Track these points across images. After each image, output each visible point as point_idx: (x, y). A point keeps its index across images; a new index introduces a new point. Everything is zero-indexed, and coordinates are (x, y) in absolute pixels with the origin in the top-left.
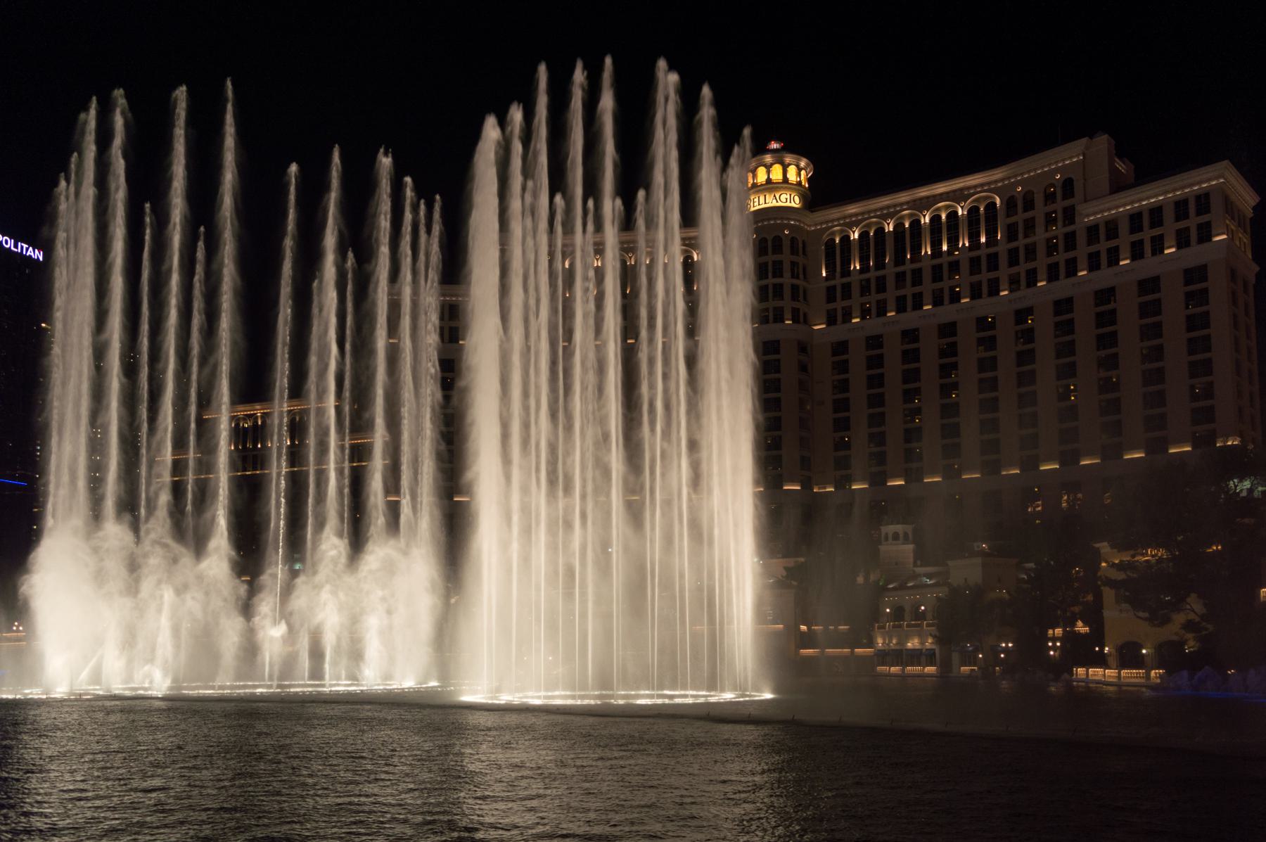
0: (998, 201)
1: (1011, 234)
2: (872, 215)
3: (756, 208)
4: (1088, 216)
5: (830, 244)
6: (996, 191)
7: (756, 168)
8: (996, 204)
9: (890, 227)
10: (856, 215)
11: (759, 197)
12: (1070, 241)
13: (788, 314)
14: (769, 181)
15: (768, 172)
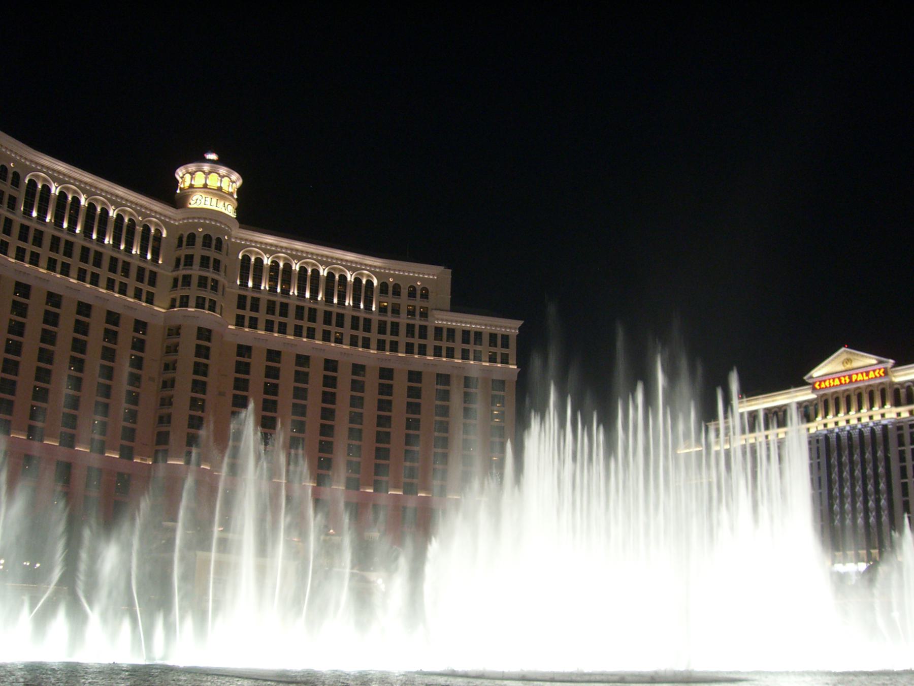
0: (375, 282)
1: (382, 310)
2: (284, 251)
3: (208, 207)
4: (438, 320)
5: (246, 259)
6: (377, 275)
7: (210, 173)
8: (372, 283)
9: (296, 267)
10: (271, 245)
11: (211, 198)
12: (423, 331)
13: (218, 309)
14: (220, 189)
15: (221, 181)
